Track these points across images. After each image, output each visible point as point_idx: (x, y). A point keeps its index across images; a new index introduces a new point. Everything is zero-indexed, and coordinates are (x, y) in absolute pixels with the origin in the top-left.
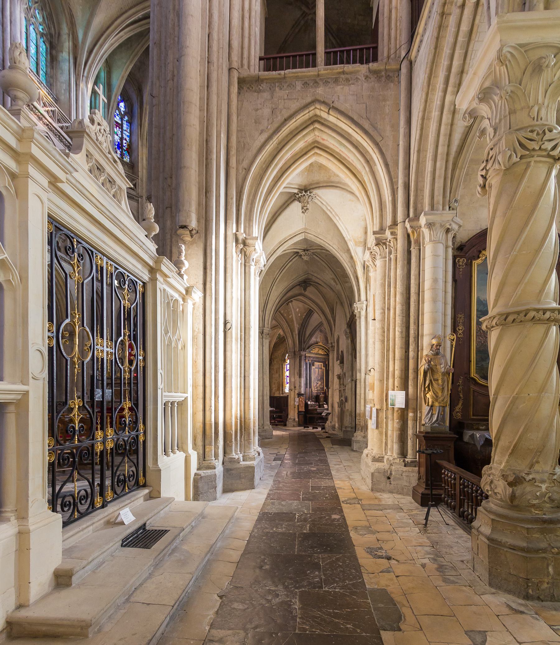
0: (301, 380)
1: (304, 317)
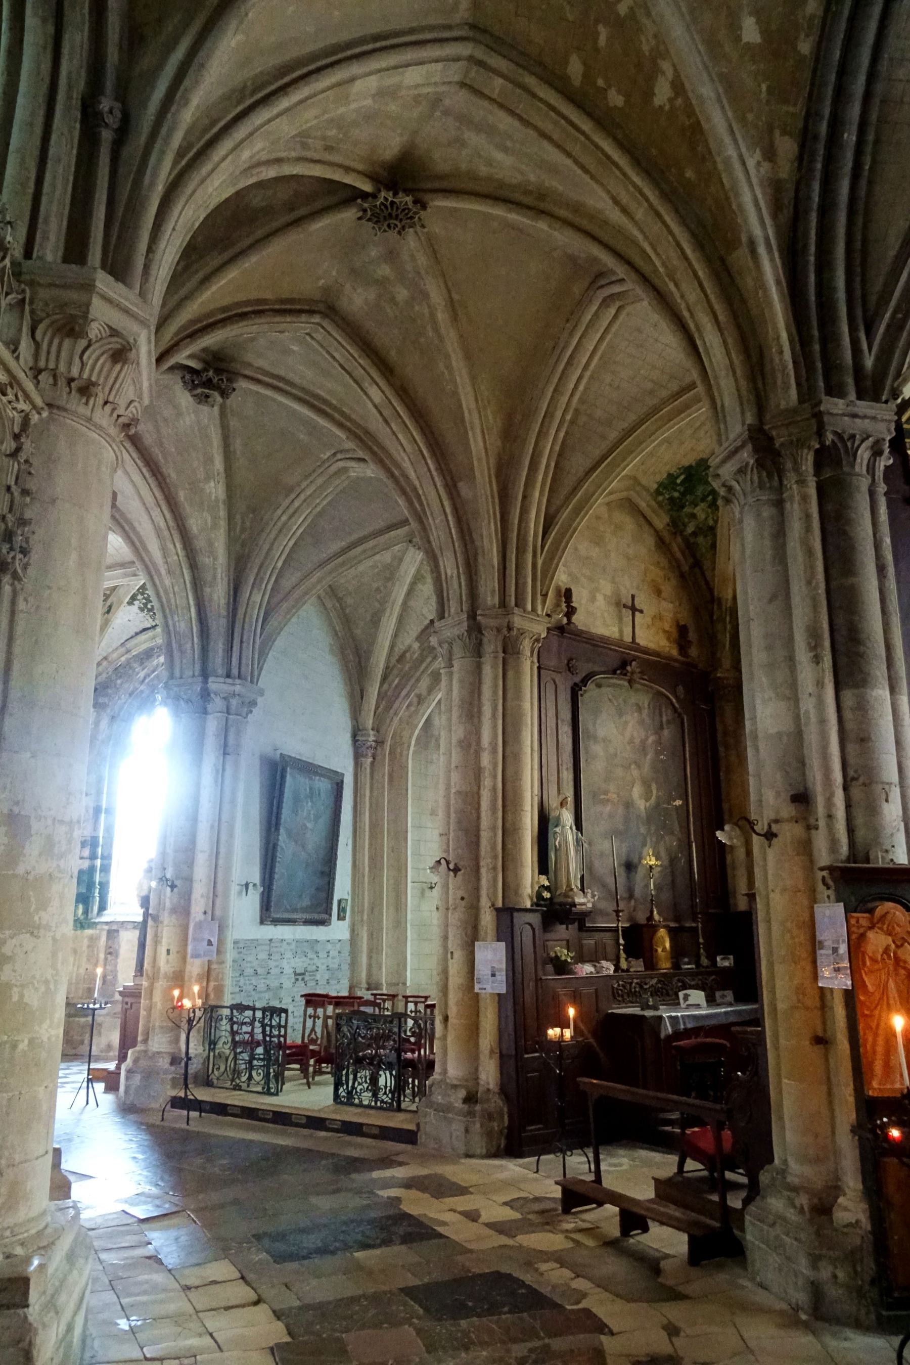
0: (862, 707)
1: (805, 47)
